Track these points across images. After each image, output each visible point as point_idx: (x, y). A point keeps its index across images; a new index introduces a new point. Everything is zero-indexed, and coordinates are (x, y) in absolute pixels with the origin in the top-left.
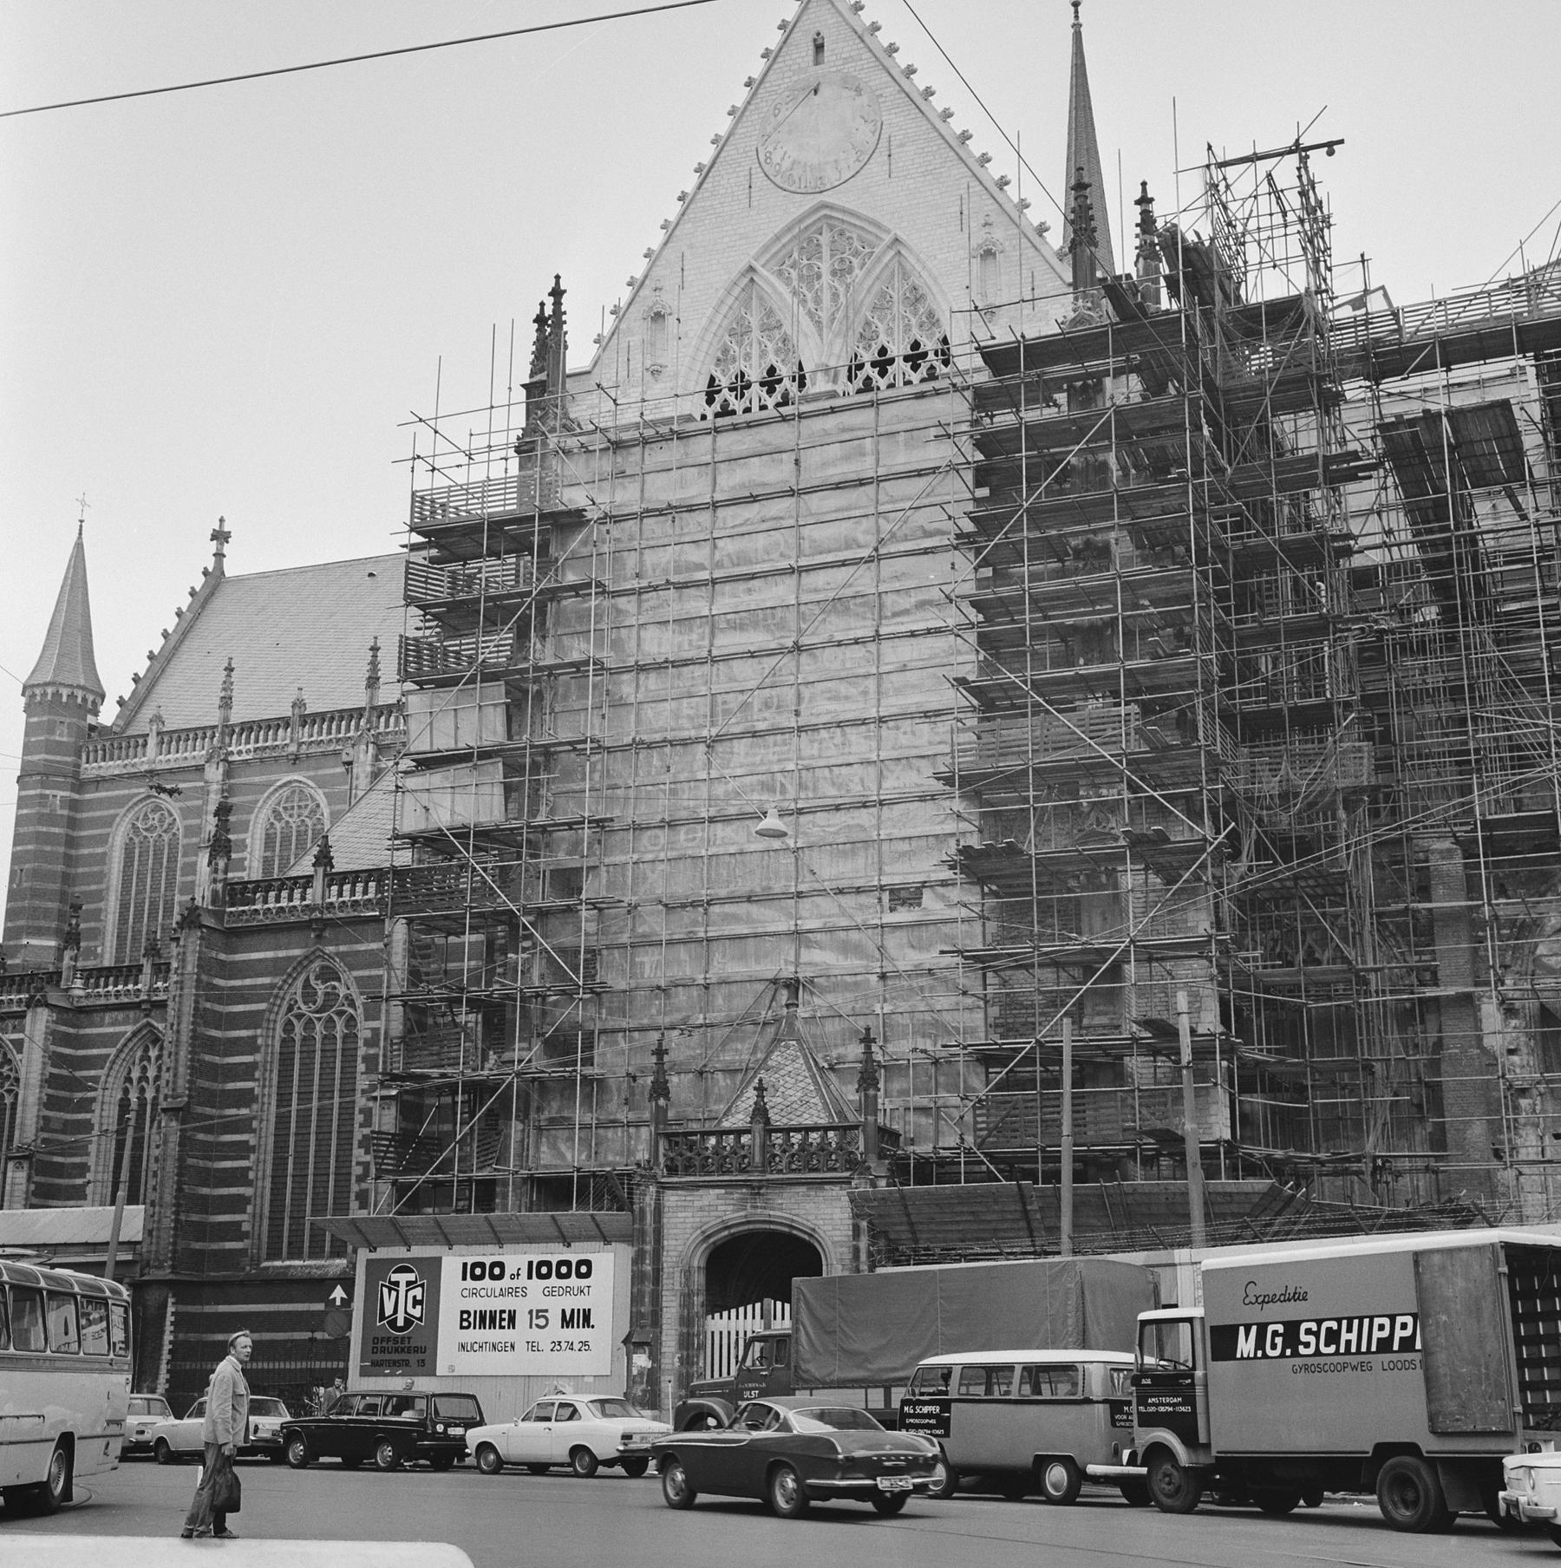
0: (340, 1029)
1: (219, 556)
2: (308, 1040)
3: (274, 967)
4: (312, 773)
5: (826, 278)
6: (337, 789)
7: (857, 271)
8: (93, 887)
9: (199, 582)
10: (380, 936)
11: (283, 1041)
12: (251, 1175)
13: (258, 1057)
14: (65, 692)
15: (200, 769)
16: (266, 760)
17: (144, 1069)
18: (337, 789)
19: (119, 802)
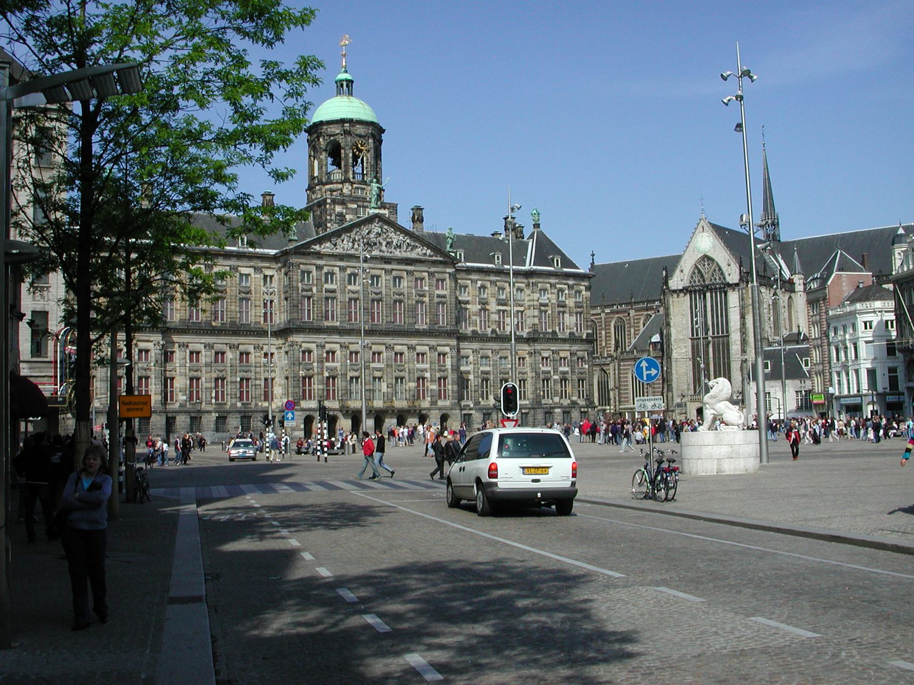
3: (630, 365)
16: (612, 312)
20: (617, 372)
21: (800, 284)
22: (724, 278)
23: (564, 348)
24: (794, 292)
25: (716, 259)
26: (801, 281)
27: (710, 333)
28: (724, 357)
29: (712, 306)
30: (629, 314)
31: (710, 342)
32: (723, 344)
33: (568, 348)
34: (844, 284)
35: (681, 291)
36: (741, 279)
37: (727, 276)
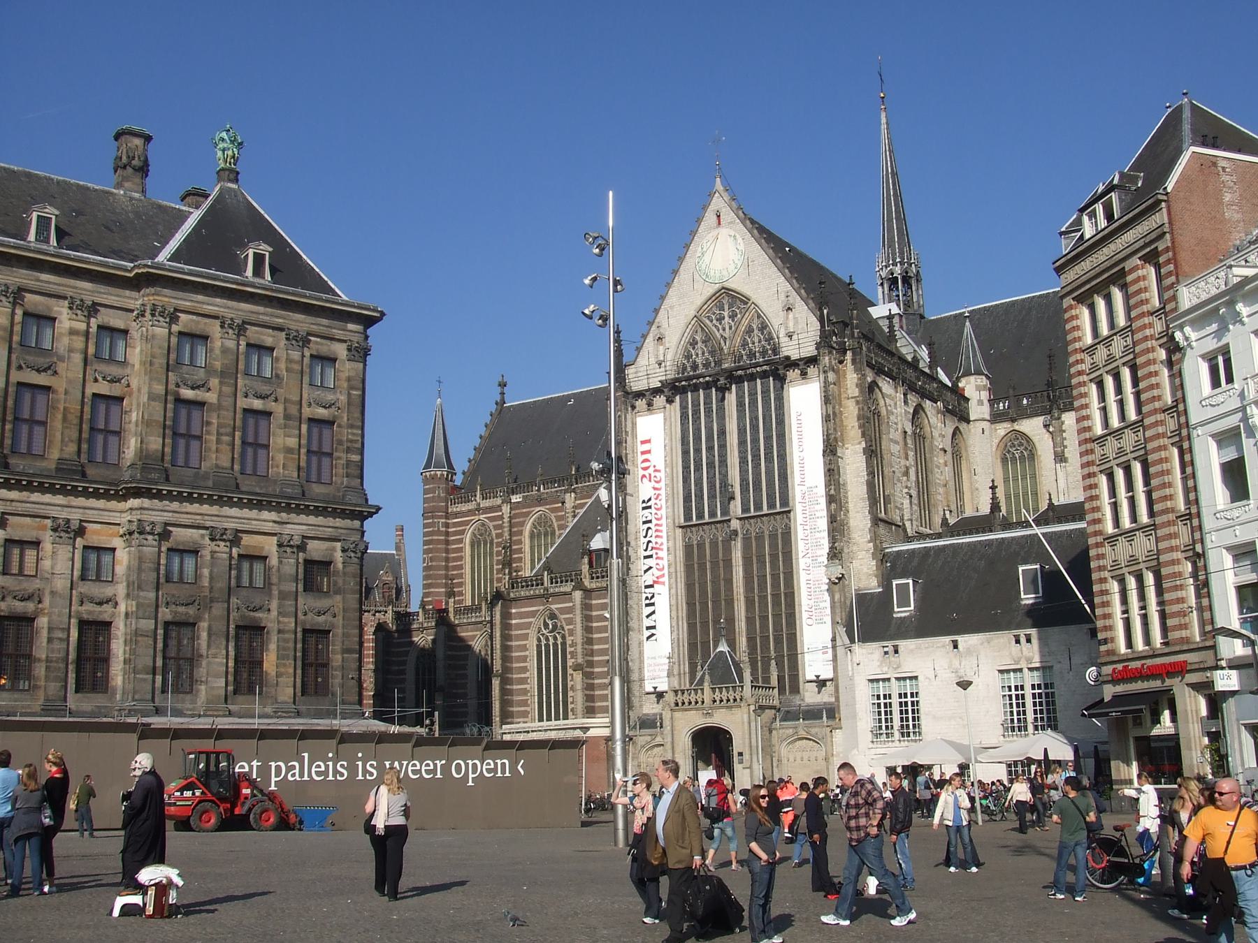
0: (559, 641)
1: (502, 394)
2: (547, 646)
3: (533, 614)
4: (548, 507)
5: (727, 318)
6: (560, 514)
7: (739, 316)
8: (459, 563)
9: (493, 408)
10: (571, 600)
11: (537, 645)
12: (529, 702)
13: (527, 653)
14: (439, 473)
15: (500, 506)
17: (487, 650)
18: (560, 514)
19: (466, 523)
20: (498, 634)
21: (980, 402)
22: (776, 350)
23: (255, 525)
24: (968, 421)
25: (754, 297)
26: (985, 395)
27: (736, 507)
28: (775, 577)
29: (742, 431)
30: (563, 503)
31: (735, 533)
32: (773, 537)
33: (269, 527)
34: (1227, 197)
35: (656, 391)
36: (824, 342)
37: (784, 340)
